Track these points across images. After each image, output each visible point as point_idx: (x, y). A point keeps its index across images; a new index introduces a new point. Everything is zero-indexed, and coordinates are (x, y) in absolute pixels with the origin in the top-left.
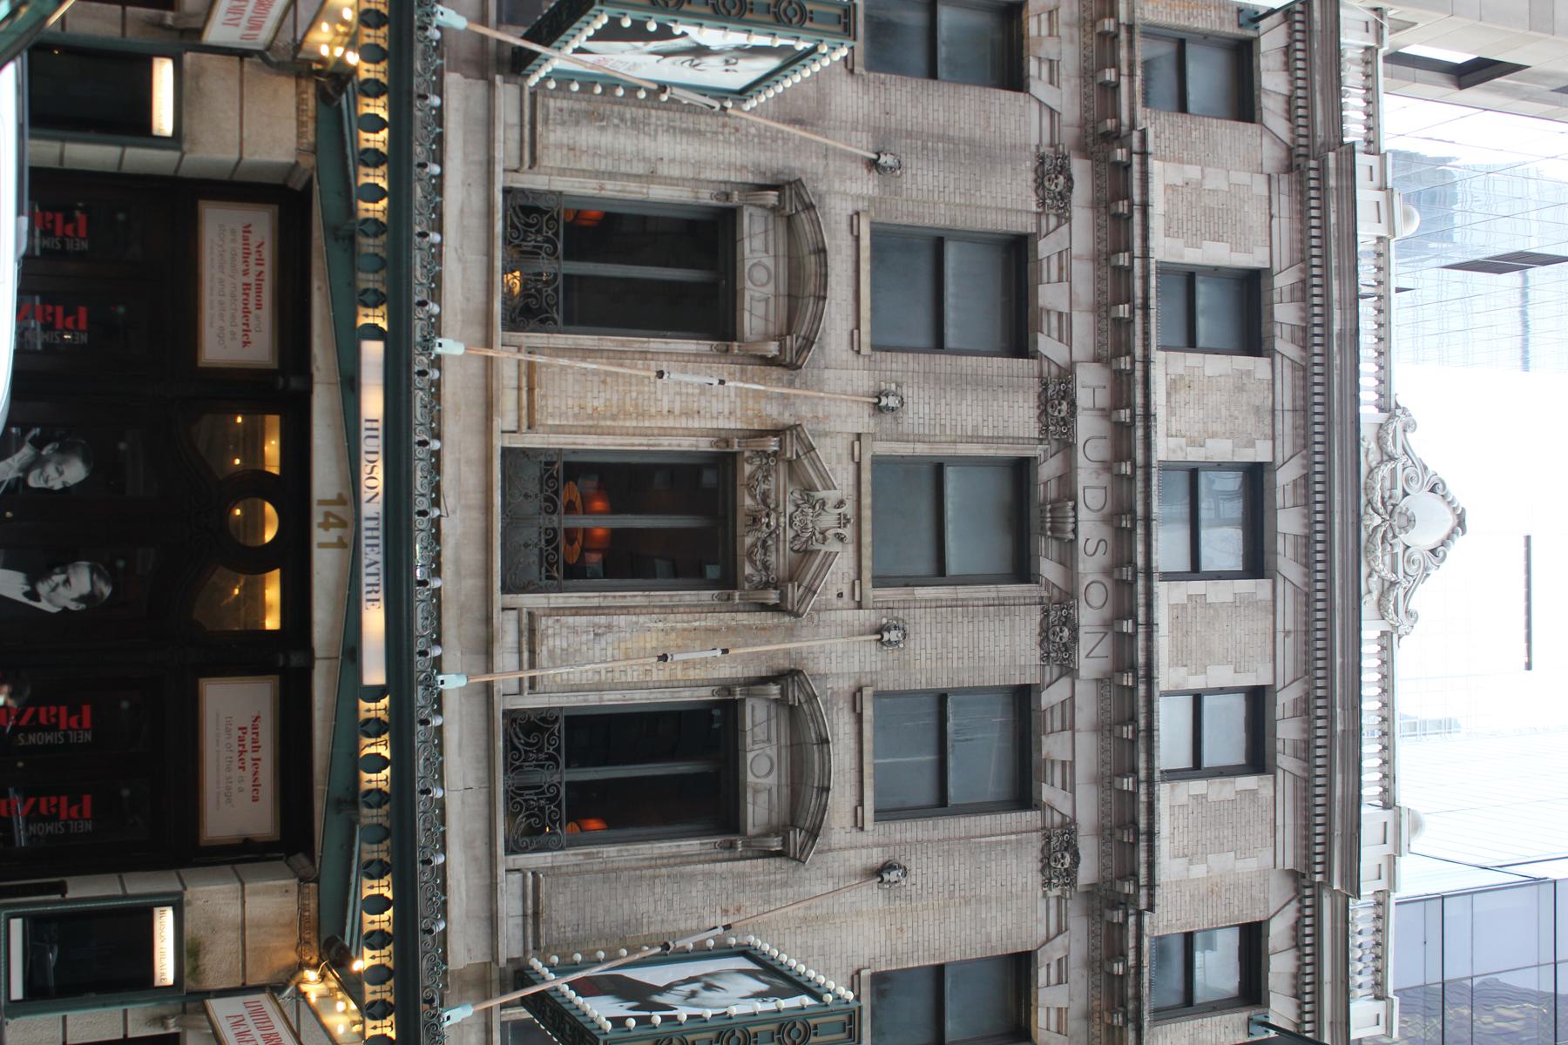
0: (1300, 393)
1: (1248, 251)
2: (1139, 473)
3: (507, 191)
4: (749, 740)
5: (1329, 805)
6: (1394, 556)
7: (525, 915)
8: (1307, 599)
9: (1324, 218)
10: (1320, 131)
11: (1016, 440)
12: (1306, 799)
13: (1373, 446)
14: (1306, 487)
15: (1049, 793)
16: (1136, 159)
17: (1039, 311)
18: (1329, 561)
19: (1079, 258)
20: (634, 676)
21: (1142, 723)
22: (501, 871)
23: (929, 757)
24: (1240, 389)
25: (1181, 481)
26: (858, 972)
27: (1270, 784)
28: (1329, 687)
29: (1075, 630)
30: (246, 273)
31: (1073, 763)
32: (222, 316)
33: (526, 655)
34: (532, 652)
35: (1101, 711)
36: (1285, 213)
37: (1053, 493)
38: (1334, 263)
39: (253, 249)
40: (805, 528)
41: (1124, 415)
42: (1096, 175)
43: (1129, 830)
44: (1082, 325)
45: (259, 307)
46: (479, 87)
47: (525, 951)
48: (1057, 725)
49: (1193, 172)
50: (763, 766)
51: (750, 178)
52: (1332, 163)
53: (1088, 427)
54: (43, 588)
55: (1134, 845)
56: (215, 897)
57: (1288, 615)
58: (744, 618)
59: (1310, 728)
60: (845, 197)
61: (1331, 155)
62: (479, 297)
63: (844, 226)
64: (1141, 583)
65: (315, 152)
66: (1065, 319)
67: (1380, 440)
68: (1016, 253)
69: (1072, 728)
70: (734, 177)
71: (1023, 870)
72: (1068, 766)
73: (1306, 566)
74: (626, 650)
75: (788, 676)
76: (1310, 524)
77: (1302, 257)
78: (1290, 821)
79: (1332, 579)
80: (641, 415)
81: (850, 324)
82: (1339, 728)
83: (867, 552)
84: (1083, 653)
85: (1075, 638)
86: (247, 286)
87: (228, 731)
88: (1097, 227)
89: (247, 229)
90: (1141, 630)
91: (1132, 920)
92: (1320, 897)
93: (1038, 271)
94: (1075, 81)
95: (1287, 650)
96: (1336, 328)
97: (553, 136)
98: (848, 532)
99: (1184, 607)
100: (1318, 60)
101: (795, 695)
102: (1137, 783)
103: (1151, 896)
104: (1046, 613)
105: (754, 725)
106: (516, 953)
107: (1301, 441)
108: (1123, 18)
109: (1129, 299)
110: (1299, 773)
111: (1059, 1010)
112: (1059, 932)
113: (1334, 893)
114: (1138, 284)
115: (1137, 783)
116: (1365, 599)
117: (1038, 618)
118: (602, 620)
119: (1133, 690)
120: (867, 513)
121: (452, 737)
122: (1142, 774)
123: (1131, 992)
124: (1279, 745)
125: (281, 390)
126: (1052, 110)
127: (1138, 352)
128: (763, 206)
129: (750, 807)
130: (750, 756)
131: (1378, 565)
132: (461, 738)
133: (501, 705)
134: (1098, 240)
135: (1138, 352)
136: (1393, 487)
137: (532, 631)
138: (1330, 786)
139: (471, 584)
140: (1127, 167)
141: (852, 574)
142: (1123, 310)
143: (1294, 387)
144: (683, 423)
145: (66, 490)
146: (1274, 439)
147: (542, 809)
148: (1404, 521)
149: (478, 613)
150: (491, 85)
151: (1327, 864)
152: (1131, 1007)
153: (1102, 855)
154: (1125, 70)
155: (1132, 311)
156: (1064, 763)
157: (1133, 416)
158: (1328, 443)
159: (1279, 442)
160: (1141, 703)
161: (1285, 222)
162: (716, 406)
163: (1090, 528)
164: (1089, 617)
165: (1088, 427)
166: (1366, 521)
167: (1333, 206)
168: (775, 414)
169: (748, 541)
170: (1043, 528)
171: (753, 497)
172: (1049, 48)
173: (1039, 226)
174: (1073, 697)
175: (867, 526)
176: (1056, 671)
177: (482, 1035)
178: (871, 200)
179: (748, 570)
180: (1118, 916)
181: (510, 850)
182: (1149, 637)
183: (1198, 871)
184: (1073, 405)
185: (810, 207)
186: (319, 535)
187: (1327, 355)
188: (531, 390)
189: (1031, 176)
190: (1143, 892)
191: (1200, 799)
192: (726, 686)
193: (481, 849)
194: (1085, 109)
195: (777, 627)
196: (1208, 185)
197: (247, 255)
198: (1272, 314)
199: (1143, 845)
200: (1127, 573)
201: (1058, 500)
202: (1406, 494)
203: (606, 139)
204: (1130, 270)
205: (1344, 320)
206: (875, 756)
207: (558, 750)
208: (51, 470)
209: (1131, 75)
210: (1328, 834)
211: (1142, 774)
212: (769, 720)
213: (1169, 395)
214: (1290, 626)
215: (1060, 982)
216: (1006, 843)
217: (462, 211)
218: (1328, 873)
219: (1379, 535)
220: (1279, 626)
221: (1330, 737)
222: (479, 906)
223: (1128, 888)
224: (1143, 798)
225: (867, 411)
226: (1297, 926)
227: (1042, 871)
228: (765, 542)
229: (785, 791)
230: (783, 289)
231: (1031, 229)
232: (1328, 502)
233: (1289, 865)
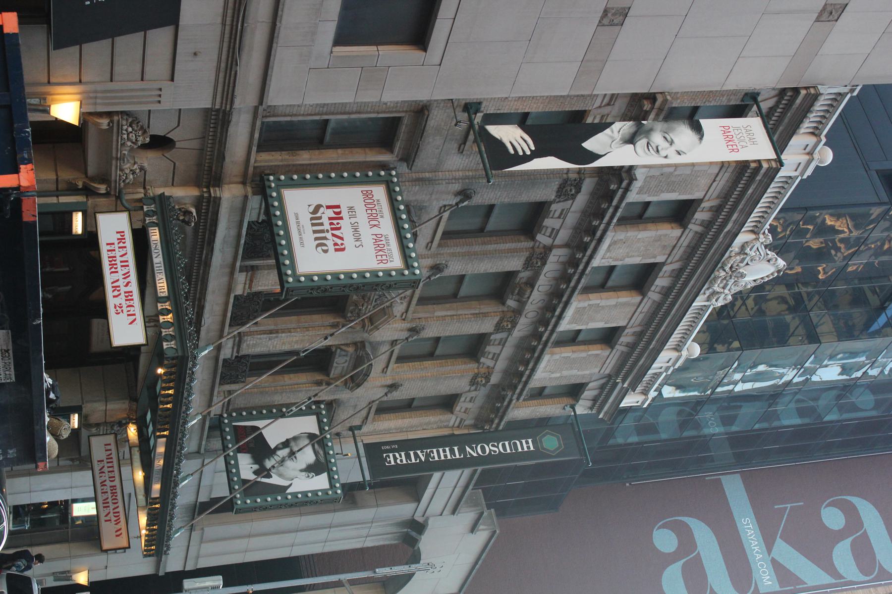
0: (694, 242)
2: (569, 290)
15: (482, 360)
21: (536, 355)
22: (215, 393)
31: (499, 355)
37: (524, 280)
38: (740, 207)
44: (564, 236)
52: (763, 171)
56: (97, 409)
64: (553, 320)
66: (554, 233)
67: (743, 247)
75: (360, 345)
77: (725, 196)
78: (613, 362)
81: (429, 240)
82: (651, 347)
95: (639, 318)
96: (726, 230)
100: (786, 120)
102: (526, 369)
106: (219, 412)
113: (622, 388)
146: (669, 255)
161: (723, 182)
166: (716, 273)
169: (351, 308)
179: (349, 315)
181: (220, 384)
193: (207, 392)
196: (676, 173)
198: (694, 214)
200: (548, 315)
201: (526, 283)
202: (747, 264)
205: (733, 227)
213: (610, 246)
214: (645, 310)
218: (624, 381)
220: (639, 310)
233: (607, 372)
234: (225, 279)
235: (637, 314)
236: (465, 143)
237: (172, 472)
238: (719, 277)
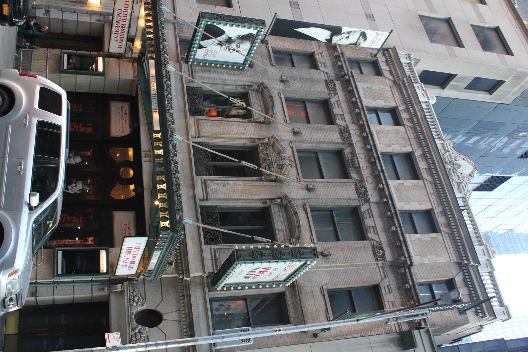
1: (389, 102)
2: (373, 147)
3: (187, 87)
4: (274, 216)
5: (461, 239)
6: (458, 176)
7: (212, 259)
8: (434, 184)
9: (407, 92)
10: (400, 76)
11: (336, 143)
12: (454, 240)
13: (441, 148)
14: (425, 156)
15: (370, 235)
16: (351, 78)
17: (334, 115)
18: (437, 172)
19: (342, 102)
20: (236, 196)
21: (393, 211)
23: (331, 229)
24: (398, 133)
25: (388, 158)
26: (322, 287)
27: (441, 236)
28: (449, 206)
29: (366, 189)
30: (122, 116)
31: (375, 226)
32: (116, 126)
33: (204, 189)
34: (206, 189)
35: (380, 211)
36: (397, 93)
37: (350, 156)
39: (124, 111)
40: (280, 162)
41: (364, 134)
42: (342, 84)
43: (399, 246)
44: (347, 117)
45: (126, 124)
46: (178, 64)
47: (213, 270)
48: (368, 216)
49: (369, 85)
50: (280, 223)
51: (250, 84)
53: (355, 139)
54: (69, 187)
55: (401, 246)
57: (430, 189)
58: (266, 183)
59: (447, 219)
60: (276, 88)
61: (405, 79)
62: (182, 106)
63: (277, 95)
65: (138, 77)
67: (443, 147)
68: (325, 105)
69: (373, 217)
70: (246, 84)
71: (368, 256)
72: (374, 227)
73: (432, 176)
74: (235, 192)
76: (429, 165)
78: (451, 246)
79: (440, 178)
80: (229, 134)
81: (283, 116)
82: (456, 216)
83: (299, 169)
84: (370, 195)
85: (367, 191)
86: (123, 119)
87: (121, 225)
88: (345, 95)
89: (122, 107)
90: (385, 186)
91: (407, 270)
92: (469, 269)
93: (332, 106)
94: (331, 68)
96: (419, 116)
97: (197, 74)
98: (293, 164)
99: (398, 186)
100: (394, 61)
101: (285, 201)
103: (410, 260)
104: (356, 185)
105: (275, 213)
107: (419, 145)
108: (339, 51)
109: (358, 107)
110: (449, 232)
111: (392, 302)
112: (385, 278)
114: (359, 104)
115: (396, 227)
116: (455, 190)
117: (354, 186)
118: (225, 182)
119: (387, 203)
120: (297, 160)
121: (185, 208)
122: (397, 225)
123: (414, 293)
124: (440, 225)
125: (133, 140)
126: (327, 73)
127: (364, 119)
128: (254, 90)
129: (278, 235)
130: (275, 221)
131: (454, 178)
132: (188, 210)
133: (199, 203)
134: (346, 98)
135: (364, 119)
136: (451, 158)
137: (205, 184)
138: (459, 233)
139: (187, 171)
140: (349, 80)
141: (296, 175)
142: (357, 110)
143: (413, 133)
144: (241, 136)
145: (76, 164)
147: (214, 234)
148: (457, 166)
149: (189, 178)
150: (180, 64)
151: (467, 256)
152: (415, 298)
153: (392, 252)
154: (343, 62)
155: (360, 110)
156: (373, 227)
157: (367, 134)
158: (427, 143)
159: (413, 146)
160: (391, 205)
161: (398, 96)
162: (249, 132)
163: (363, 163)
164: (369, 185)
165: (355, 139)
166: (446, 167)
167: (409, 90)
168: (266, 134)
170: (349, 165)
171: (264, 154)
172: (323, 60)
173: (329, 96)
174: (370, 208)
175: (298, 163)
176: (363, 202)
177: (203, 300)
178: (283, 90)
180: (402, 270)
182: (388, 188)
183: (426, 261)
184: (350, 134)
185: (266, 88)
186: (143, 159)
187: (419, 123)
188: (198, 127)
189: (324, 85)
190: (408, 259)
191: (420, 239)
192: (265, 201)
193: (197, 240)
194: (336, 73)
195: (276, 186)
197: (122, 113)
199: (403, 245)
203: (211, 75)
204: (356, 102)
205: (421, 114)
206: (315, 228)
207: (217, 217)
208: (72, 159)
209: (345, 63)
210: (464, 248)
211: (397, 225)
212: (279, 211)
213: (377, 135)
214: (432, 192)
215: (390, 293)
216: (360, 247)
217: (176, 88)
218: (468, 259)
219: (451, 170)
221: (454, 219)
222: (198, 257)
223: (403, 258)
224: (399, 232)
225: (291, 134)
226: (464, 279)
227: (374, 256)
228: (269, 166)
229: (288, 230)
230: (263, 108)
231: (328, 97)
232: (432, 158)
233: (455, 260)
234: (183, 121)
235: (430, 195)
236: (271, 60)
237: (165, 102)
238: (450, 169)
